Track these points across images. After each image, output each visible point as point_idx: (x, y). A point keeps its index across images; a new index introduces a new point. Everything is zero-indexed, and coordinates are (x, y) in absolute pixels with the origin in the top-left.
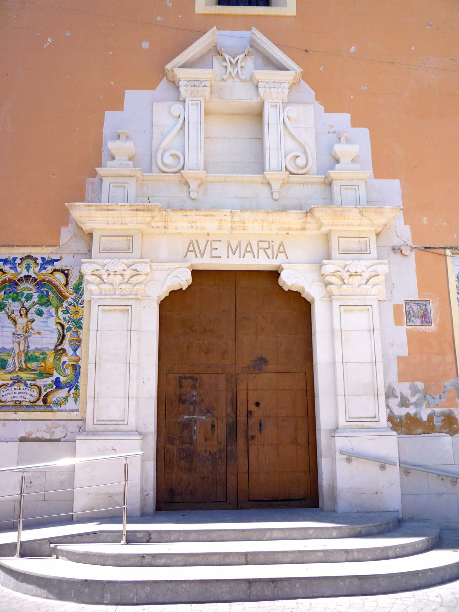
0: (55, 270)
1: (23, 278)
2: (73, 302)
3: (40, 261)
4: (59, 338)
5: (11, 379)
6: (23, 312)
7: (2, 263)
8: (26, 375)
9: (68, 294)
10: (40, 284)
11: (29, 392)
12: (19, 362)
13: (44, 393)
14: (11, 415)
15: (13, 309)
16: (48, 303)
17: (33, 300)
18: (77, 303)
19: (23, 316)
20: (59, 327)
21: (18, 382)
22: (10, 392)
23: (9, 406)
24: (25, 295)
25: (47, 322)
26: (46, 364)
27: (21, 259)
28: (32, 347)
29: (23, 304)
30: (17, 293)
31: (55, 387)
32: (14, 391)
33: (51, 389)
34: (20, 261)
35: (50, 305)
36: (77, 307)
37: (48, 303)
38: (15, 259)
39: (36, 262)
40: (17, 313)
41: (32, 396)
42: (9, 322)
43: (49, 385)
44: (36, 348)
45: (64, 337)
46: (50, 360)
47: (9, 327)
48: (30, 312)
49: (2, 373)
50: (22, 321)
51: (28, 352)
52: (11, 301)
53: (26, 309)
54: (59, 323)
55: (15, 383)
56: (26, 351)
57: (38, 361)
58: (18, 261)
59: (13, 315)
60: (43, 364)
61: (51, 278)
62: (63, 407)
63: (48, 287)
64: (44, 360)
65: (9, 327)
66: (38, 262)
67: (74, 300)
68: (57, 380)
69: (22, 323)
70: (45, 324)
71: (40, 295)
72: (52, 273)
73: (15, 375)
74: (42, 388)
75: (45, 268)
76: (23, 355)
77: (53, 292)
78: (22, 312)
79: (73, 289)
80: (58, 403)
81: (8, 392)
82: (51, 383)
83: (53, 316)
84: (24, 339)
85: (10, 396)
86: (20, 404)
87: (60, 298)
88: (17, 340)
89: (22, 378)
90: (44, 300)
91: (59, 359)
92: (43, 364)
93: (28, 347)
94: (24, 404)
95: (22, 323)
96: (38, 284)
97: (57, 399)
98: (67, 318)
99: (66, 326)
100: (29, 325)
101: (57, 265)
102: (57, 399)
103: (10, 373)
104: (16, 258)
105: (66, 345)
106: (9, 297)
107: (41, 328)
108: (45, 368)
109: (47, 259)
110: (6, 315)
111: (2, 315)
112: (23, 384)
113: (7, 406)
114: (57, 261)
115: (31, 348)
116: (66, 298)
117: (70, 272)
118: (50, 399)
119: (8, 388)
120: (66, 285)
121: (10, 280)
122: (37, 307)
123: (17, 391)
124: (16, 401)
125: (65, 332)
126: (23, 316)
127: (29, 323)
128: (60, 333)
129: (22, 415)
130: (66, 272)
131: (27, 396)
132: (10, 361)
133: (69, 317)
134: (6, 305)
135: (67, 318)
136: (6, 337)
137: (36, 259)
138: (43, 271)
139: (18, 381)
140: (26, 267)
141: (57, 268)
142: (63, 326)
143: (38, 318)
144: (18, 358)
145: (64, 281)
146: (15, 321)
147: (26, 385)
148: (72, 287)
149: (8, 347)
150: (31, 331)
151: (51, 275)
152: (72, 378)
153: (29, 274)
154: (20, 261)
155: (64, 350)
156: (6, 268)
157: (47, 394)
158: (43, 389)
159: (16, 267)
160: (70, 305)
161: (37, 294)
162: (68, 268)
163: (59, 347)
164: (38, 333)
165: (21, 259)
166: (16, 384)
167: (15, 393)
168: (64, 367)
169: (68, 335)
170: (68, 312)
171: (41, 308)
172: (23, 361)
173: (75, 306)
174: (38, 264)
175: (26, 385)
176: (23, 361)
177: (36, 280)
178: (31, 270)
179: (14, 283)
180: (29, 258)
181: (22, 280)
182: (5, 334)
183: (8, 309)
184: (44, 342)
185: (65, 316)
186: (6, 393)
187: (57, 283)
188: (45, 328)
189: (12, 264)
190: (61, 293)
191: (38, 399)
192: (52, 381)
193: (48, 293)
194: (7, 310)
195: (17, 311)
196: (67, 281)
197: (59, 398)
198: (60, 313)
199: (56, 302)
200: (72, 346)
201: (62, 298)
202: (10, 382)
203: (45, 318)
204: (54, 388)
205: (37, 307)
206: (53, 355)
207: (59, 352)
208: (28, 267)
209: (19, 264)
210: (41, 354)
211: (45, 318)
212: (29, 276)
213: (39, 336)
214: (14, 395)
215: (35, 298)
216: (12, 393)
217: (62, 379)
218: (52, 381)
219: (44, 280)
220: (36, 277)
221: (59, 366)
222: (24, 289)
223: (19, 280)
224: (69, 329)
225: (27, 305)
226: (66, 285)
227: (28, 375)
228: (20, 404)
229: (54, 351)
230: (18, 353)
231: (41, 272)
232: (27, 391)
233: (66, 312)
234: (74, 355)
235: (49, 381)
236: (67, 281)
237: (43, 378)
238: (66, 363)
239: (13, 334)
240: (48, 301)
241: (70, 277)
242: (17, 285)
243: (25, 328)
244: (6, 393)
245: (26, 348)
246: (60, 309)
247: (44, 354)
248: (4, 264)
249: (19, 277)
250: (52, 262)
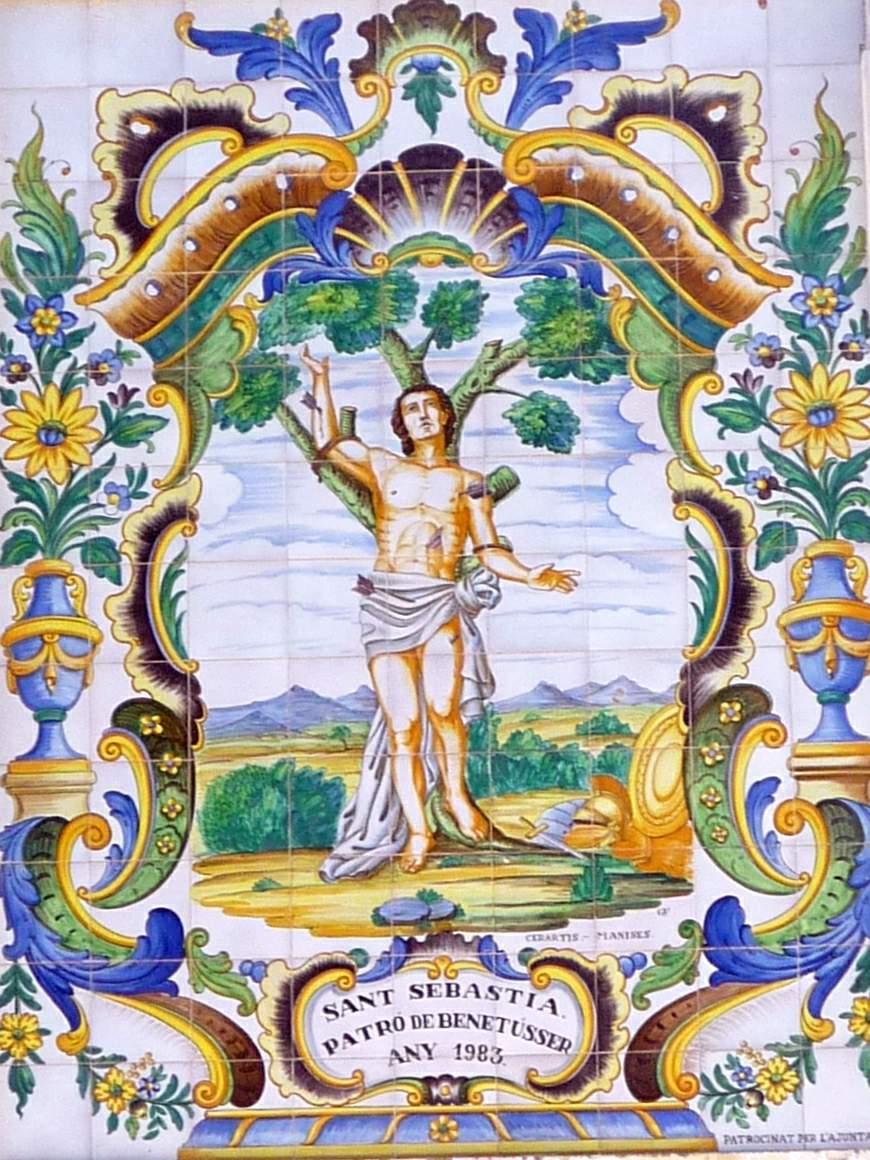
0: (631, 106)
1: (400, 173)
2: (786, 337)
3: (508, 42)
4: (710, 607)
5: (379, 920)
6: (423, 421)
7: (232, 60)
8: (486, 891)
9: (743, 284)
10: (528, 209)
11: (517, 1011)
12: (424, 797)
13: (630, 1021)
15: (342, 400)
16: (605, 353)
17: (486, 333)
18: (820, 345)
19: (428, 452)
20: (705, 531)
21: (432, 942)
22: (383, 1013)
23: (385, 1117)
24: (423, 299)
25: (608, 491)
26: (626, 808)
27: (365, 29)
28: (514, 682)
29: (417, 367)
30: (361, 284)
31: (707, 969)
32: (405, 1005)
33: (681, 990)
34: (360, 48)
35: (622, 367)
36: (819, 378)
37: (605, 353)
38: (322, 30)
39: (481, 49)
40: (376, 432)
41: (546, 1039)
42: (323, 505)
43: (665, 957)
44: (548, 688)
45: (741, 597)
46: (658, 774)
47: (328, 538)
48: (471, 422)
49: (312, 879)
50: (419, 493)
51: (484, 715)
52: (320, 343)
53: (443, 400)
54: (703, 501)
55: (411, 946)
56: (472, 711)
57: (563, 786)
58: (348, 47)
59: (347, 446)
60: (607, 806)
61: (602, 163)
62: (783, 1117)
63: (590, 231)
64: (610, 774)
65: (328, 538)
66: (494, 45)
67: (795, 322)
68: (721, 926)
69: (422, 507)
70: (595, 511)
71: (532, 293)
72: (607, 130)
73: (408, 889)
74: (616, 978)
75: (555, 93)
76: (452, 739)
77: (631, 272)
78: (411, 420)
79: (783, 242)
80: (740, 1090)
81: (368, 1016)
82: (678, 942)
83: (652, 449)
84: (451, 623)
85: (382, 1045)
86: (463, 1099)
87: (693, 315)
88: (397, 632)
89: (457, 912)
90: (570, 331)
91: (724, 768)
92: (607, 806)
93: (486, 683)
94: (490, 1097)
95: (422, 507)
96: (511, 210)
97: (733, 1063)
98: (757, 462)
99: (756, 517)
100: (478, 519)
101: (643, 68)
102: (733, 1063)
103: (367, 876)
104: (333, 22)
105: (763, 659)
106: (308, 317)
107: (566, 539)
108: (623, 836)
109: (561, 22)
110: (296, 453)
111: (273, 451)
112: (472, 956)
113: (364, 1119)
114: (637, 33)
115: (502, 694)
116: (733, 308)
117: (746, 115)
118: (676, 1060)
119: (364, 990)
120: (727, 211)
121: (300, 190)
122: (524, 379)
123: (425, 1006)
124: (429, 1081)
125: (750, 560)
126: (428, 452)
127: (475, 505)
128: (703, 561)
130: (717, 115)
131: (507, 1042)
132: (361, 789)
133: (770, 454)
134: (290, 376)
135: (757, 462)
136: (317, 610)
137: (479, 27)
138: (545, 117)
139: (430, 930)
140: (410, 91)
141: (644, 90)
142: (728, 523)
143: (533, 466)
144: (417, 763)
145: (704, 188)
146: (365, 493)
147: (494, 963)
148: (772, 228)
149: (338, 683)
150: (497, 561)
151: (601, 143)
152: (835, 906)
153: (441, 139)
154: (360, 48)
155: (754, 701)
156: (267, 100)
157: (654, 1022)
158: (621, 989)
159: (334, 91)
160: (769, 361)
161: (516, 286)
162: (729, 88)
163: (717, 680)
164: (547, 575)
165: (365, 29)
166: (419, 955)
167: (421, 1022)
168: (767, 824)
169: (773, 582)
170: (756, 415)
171: (552, 389)
172: (453, 783)
173: (805, 372)
174: (497, 64)
175: (494, 963)
176: (453, 783)
177: (492, 181)
178: (452, 110)
179: (337, 211)
180: (426, 22)
181: (392, 188)
182: (303, 587)
183: (310, 401)
184: (597, 641)
185: (742, 442)
186: (351, 1022)
187: (658, 201)
188: (599, 540)
189: (308, 69)
190: (692, 276)
191: (593, 1066)
192: (686, 928)
193: (591, 278)
194: (304, 414)
195: (375, 414)
196: (730, 182)
197: (745, 1048)
198: (702, 429)
199: (663, 344)
200: (810, 666)
201: (702, 310)
202: (378, 946)
203: (591, 461)
204: (702, 982)
205: (524, 379)
206: (674, 738)
207: (718, 712)
208: (427, 91)
209: (358, 69)
210: (583, 732)
211: (591, 461)
212: (446, 157)
213: (558, 598)
214: (411, 1037)
215: (503, 317)
216: (397, 1024)
217: (760, 912)
218: (686, 928)
219: (556, 182)
220: (494, 158)
221: (721, 815)
222: (412, 251)
223: (367, 187)
224: (778, 539)
225: (448, 368)
226: (727, 211)
227: (506, 892)
228: (463, 1099)
229: (676, 709)
230: (416, 726)
231: (527, 127)
232: (503, 1008)
233: (745, 410)
234: (831, 728)
235: (661, 926)
236: (730, 182)
237: (618, 910)
238: (779, 796)
239: (365, 586)
240: (604, 333)
241: (748, 152)
242: (356, 221)
243: (449, 540)
244: (351, 1022)
245: (469, 691)
246: (698, 396)
247: (602, 728)
248: (240, 74)
249: (367, 162)
250: (602, 43)
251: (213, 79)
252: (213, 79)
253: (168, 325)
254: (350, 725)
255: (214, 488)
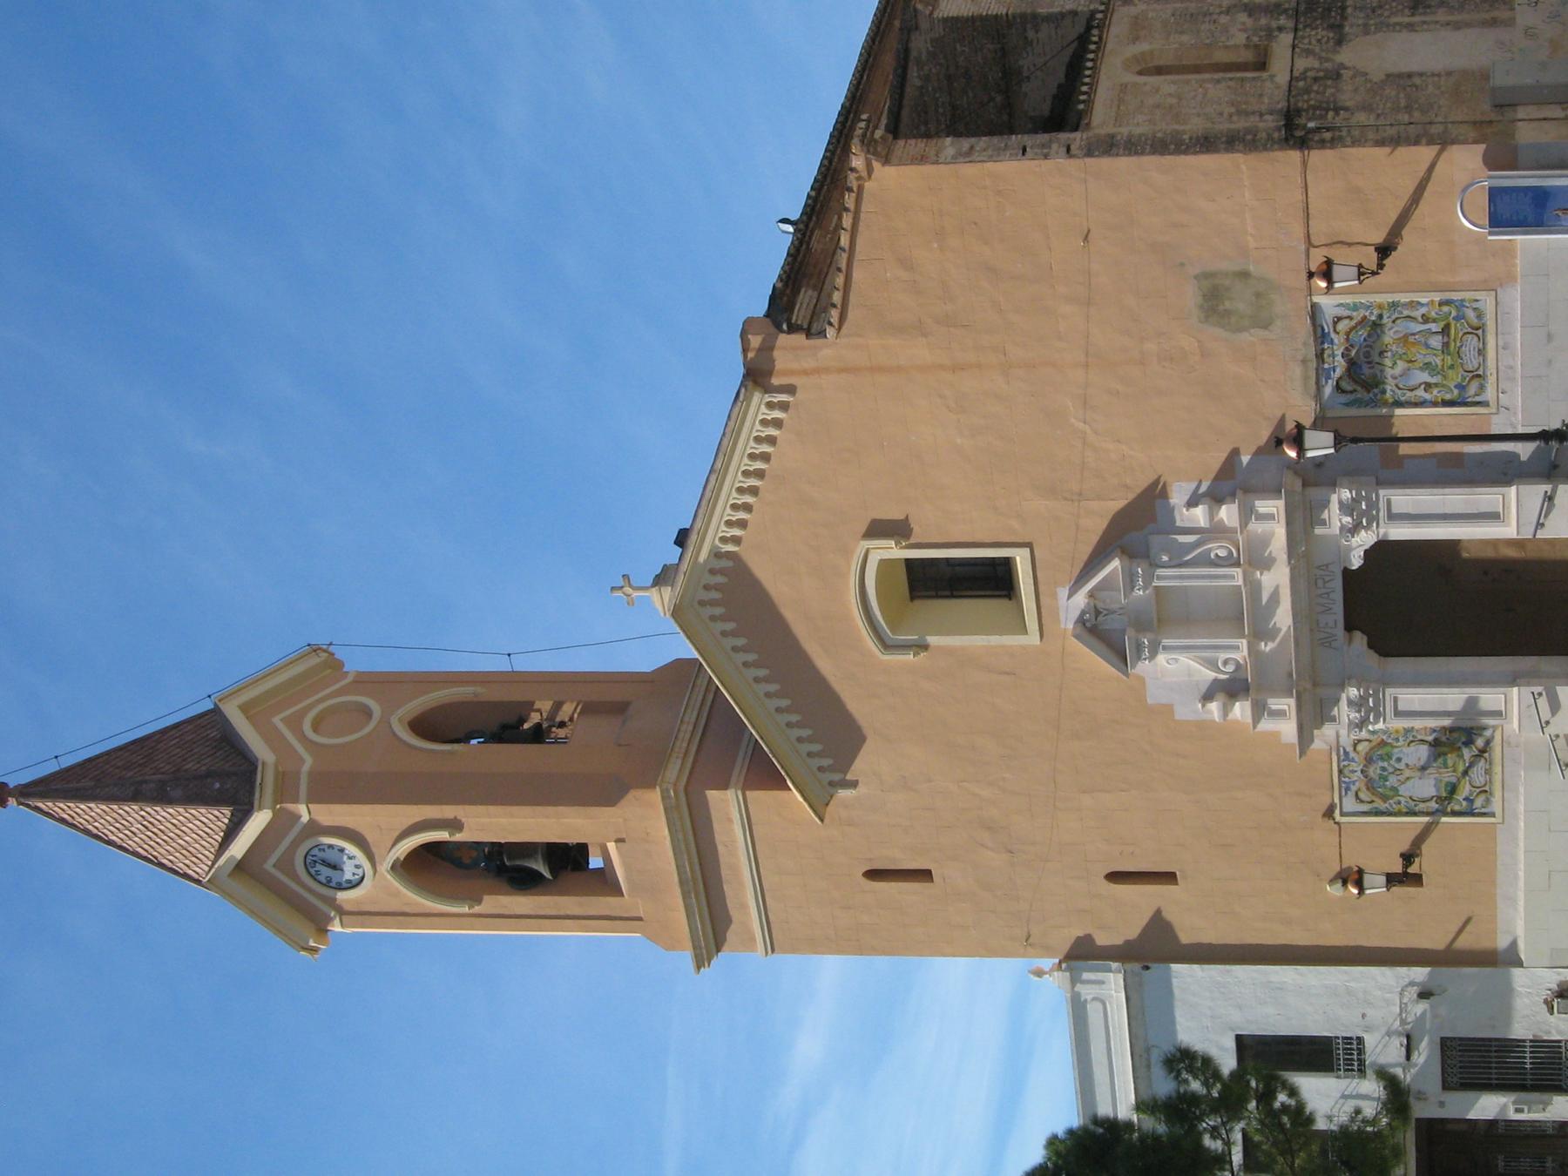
10: (1369, 760)
14: (1497, 778)
42: (1409, 783)
50: (1407, 773)
101: (1350, 749)
129: (1497, 769)
149: (1433, 782)
179: (1370, 785)
215: (1381, 764)
251: (1351, 794)
252: (1351, 794)
253: (1385, 798)
254: (1438, 781)
255: (1408, 794)
